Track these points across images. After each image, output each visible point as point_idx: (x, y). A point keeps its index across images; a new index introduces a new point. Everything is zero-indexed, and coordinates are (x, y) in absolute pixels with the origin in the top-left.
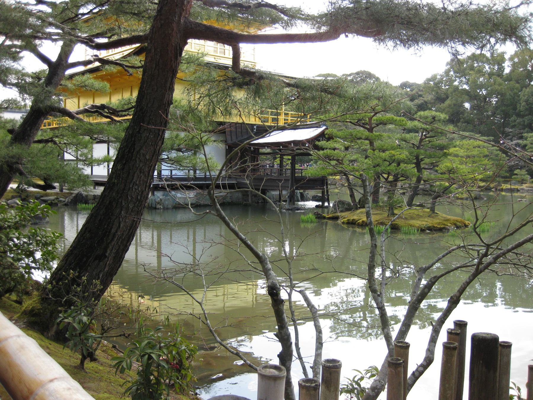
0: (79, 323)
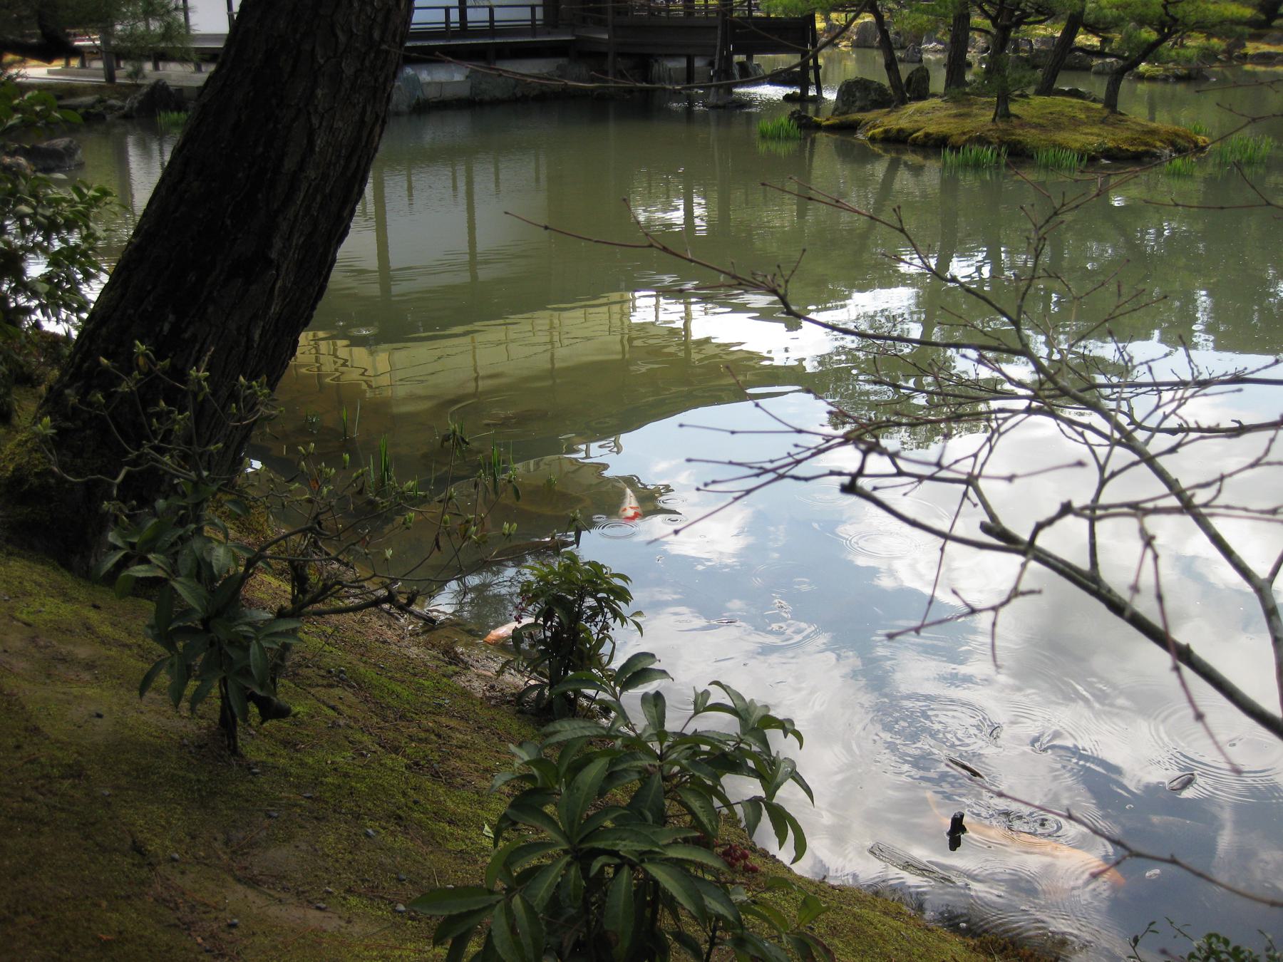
0: (198, 576)
